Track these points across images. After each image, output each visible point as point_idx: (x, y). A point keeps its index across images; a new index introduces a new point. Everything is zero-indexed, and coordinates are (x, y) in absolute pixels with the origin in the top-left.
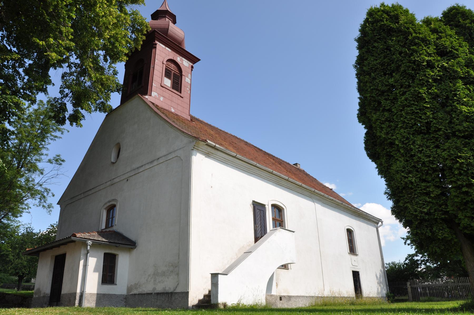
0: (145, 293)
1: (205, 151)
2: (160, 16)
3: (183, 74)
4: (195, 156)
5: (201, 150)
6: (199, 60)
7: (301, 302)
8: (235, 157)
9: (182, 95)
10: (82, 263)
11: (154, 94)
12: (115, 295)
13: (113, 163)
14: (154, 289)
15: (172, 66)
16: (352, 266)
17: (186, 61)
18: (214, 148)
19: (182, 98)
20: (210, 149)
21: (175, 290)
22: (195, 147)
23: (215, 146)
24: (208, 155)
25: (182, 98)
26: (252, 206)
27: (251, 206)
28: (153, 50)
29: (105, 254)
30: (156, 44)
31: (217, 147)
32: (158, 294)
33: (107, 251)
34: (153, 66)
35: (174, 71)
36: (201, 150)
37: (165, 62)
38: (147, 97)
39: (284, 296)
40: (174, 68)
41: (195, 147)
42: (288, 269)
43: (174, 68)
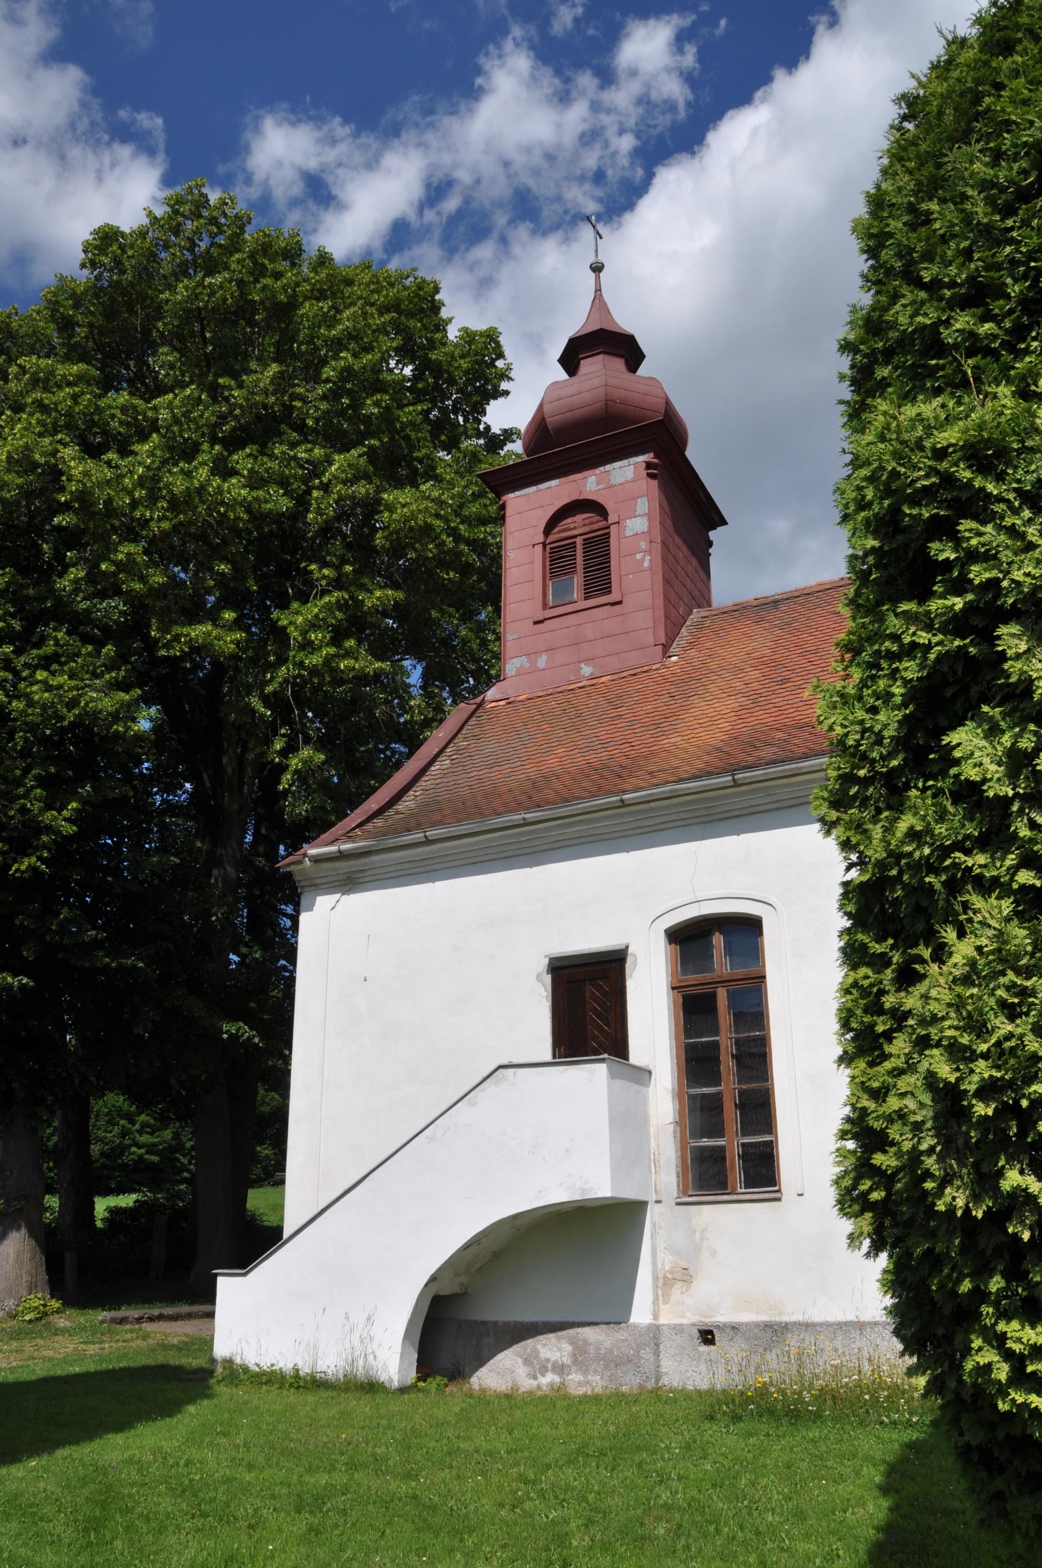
1: (336, 878)
4: (310, 909)
5: (323, 881)
8: (428, 842)
9: (614, 596)
11: (512, 666)
15: (578, 524)
17: (625, 462)
19: (620, 603)
23: (340, 851)
24: (349, 884)
25: (620, 603)
26: (548, 979)
27: (539, 978)
31: (345, 851)
35: (581, 535)
36: (323, 881)
39: (734, 1328)
40: (587, 522)
42: (779, 1199)
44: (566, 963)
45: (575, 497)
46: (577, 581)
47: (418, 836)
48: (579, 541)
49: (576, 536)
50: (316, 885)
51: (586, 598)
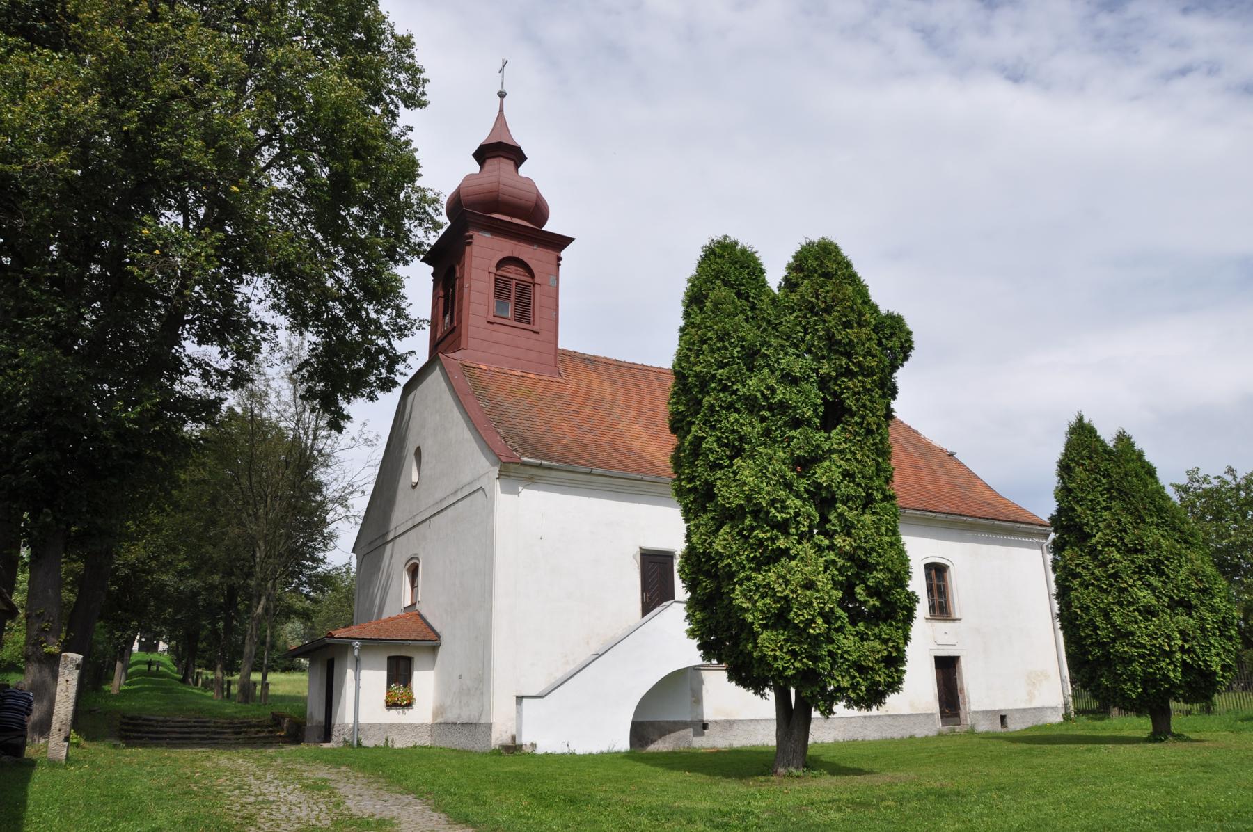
0: (450, 722)
2: (487, 155)
3: (537, 280)
6: (570, 240)
7: (762, 731)
8: (590, 473)
9: (535, 328)
10: (350, 674)
12: (411, 724)
13: (414, 487)
14: (459, 716)
15: (512, 272)
16: (936, 647)
18: (540, 466)
19: (538, 333)
20: (533, 471)
21: (479, 719)
22: (503, 473)
25: (538, 333)
27: (634, 557)
28: (468, 248)
29: (389, 658)
30: (471, 237)
32: (462, 724)
33: (393, 654)
34: (467, 285)
37: (493, 269)
38: (458, 355)
40: (518, 272)
41: (503, 473)
43: (518, 272)
44: (647, 553)
45: (515, 255)
46: (511, 306)
47: (588, 470)
48: (513, 282)
49: (512, 279)
50: (509, 476)
51: (516, 320)
